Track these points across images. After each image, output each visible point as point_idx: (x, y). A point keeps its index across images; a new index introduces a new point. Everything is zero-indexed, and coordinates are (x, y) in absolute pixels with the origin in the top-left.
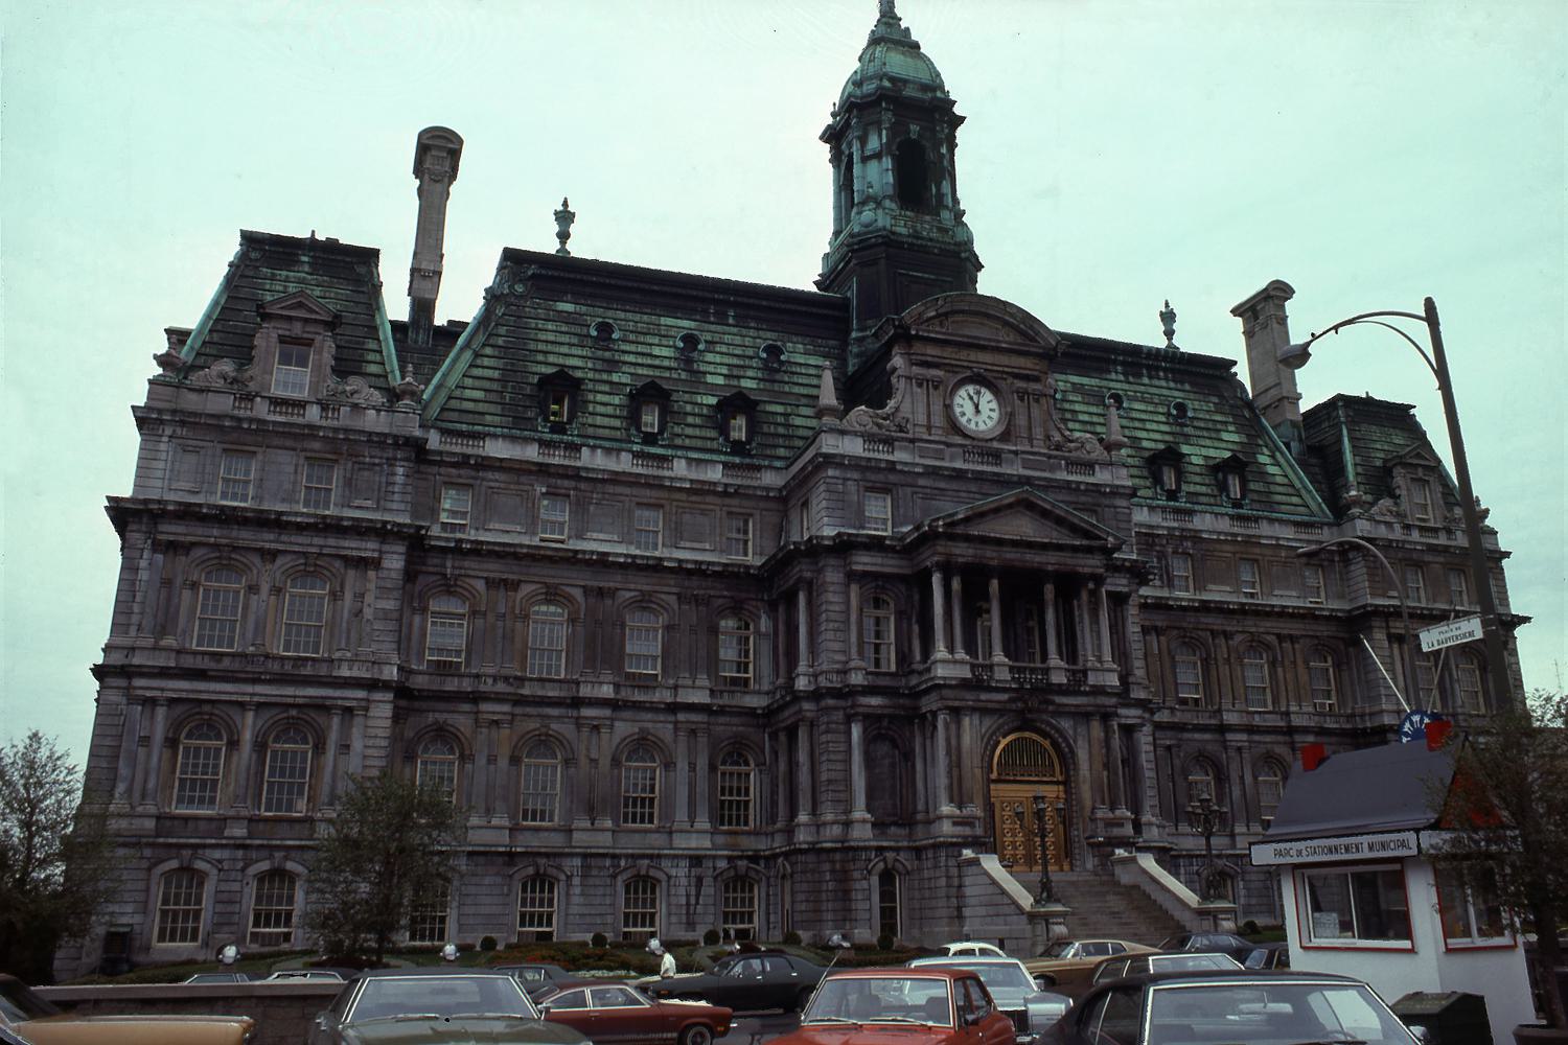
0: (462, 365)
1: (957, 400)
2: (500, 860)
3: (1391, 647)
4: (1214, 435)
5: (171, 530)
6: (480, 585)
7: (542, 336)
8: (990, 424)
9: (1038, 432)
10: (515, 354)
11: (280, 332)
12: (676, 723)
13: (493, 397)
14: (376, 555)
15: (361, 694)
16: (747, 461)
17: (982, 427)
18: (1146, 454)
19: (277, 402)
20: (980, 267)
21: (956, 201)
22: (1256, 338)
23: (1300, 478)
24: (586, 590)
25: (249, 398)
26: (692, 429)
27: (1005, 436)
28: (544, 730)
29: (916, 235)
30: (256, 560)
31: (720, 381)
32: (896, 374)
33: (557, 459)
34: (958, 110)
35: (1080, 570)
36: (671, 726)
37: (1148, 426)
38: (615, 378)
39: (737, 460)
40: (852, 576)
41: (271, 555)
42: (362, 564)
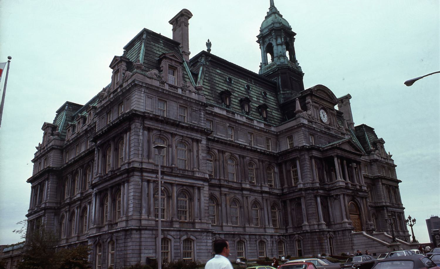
2: (231, 236)
3: (382, 186)
5: (148, 123)
6: (216, 151)
8: (326, 121)
11: (169, 63)
12: (262, 197)
13: (210, 95)
14: (200, 139)
15: (201, 183)
17: (325, 121)
19: (171, 86)
22: (342, 108)
24: (239, 156)
25: (163, 83)
27: (330, 124)
28: (235, 197)
29: (292, 67)
30: (170, 136)
31: (256, 100)
32: (309, 104)
35: (357, 160)
36: (261, 198)
40: (311, 158)
41: (173, 135)
42: (198, 141)
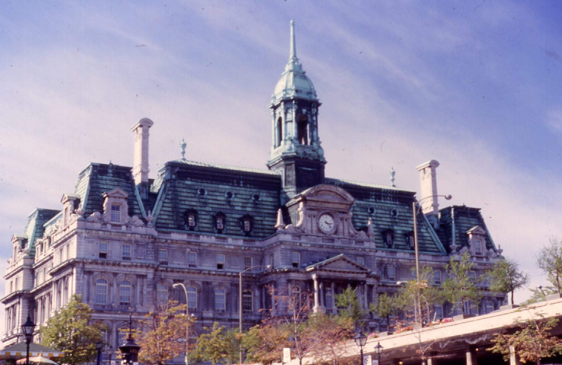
0: (160, 207)
1: (321, 221)
4: (406, 222)
7: (182, 194)
9: (346, 231)
10: (175, 200)
13: (170, 218)
16: (251, 238)
18: (381, 230)
20: (325, 163)
21: (318, 138)
23: (436, 238)
25: (105, 224)
26: (232, 227)
27: (336, 233)
31: (239, 208)
33: (193, 239)
34: (320, 102)
37: (383, 219)
38: (207, 209)
39: (247, 238)
